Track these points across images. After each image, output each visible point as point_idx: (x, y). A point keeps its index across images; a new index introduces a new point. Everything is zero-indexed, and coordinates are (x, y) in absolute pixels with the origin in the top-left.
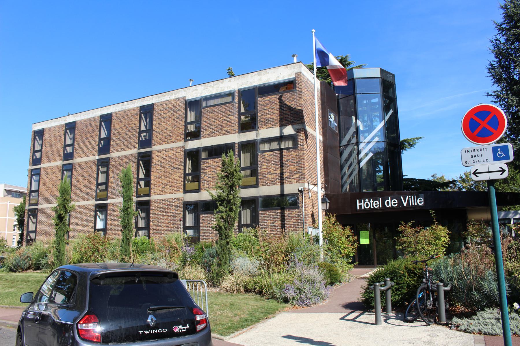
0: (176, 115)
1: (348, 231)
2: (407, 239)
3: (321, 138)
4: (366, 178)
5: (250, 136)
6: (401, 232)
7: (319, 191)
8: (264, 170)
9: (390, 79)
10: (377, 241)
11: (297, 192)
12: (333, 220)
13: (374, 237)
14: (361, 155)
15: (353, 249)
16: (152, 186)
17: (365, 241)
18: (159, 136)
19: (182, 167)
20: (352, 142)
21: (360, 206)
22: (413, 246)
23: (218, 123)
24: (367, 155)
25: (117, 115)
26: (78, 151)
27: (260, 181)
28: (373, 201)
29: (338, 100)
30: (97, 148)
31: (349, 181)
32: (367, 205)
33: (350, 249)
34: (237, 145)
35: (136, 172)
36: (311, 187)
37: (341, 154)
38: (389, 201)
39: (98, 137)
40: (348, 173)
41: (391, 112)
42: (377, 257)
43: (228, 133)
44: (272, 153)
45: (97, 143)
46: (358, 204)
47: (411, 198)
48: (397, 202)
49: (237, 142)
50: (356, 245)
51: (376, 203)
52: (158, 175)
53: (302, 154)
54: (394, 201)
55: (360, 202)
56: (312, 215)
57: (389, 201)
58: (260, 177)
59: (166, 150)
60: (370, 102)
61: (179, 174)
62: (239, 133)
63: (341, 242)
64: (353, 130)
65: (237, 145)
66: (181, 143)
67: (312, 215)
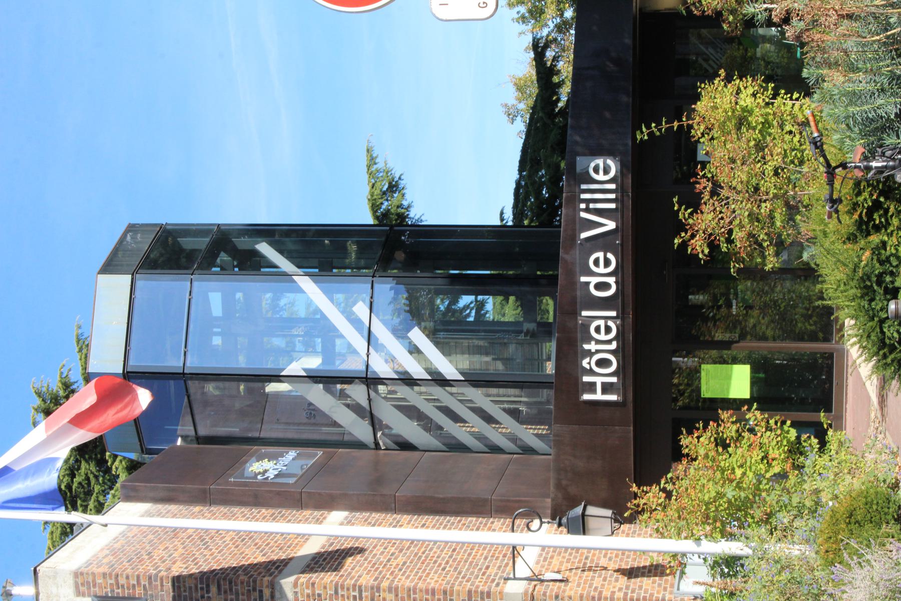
1: (698, 444)
2: (741, 226)
3: (337, 516)
4: (506, 361)
6: (713, 246)
7: (540, 539)
9: (144, 243)
10: (743, 337)
12: (652, 496)
13: (726, 345)
14: (417, 371)
15: (768, 428)
17: (738, 381)
20: (364, 403)
21: (606, 388)
22: (765, 208)
24: (414, 350)
28: (589, 339)
29: (200, 440)
31: (509, 424)
32: (602, 363)
33: (768, 437)
36: (522, 570)
37: (405, 446)
38: (594, 280)
40: (478, 424)
41: (265, 248)
42: (800, 338)
46: (599, 396)
47: (588, 201)
48: (600, 255)
50: (754, 416)
51: (598, 329)
54: (596, 262)
55: (591, 387)
56: (631, 573)
57: (594, 280)
60: (220, 321)
63: (739, 472)
64: (317, 395)
67: (631, 573)
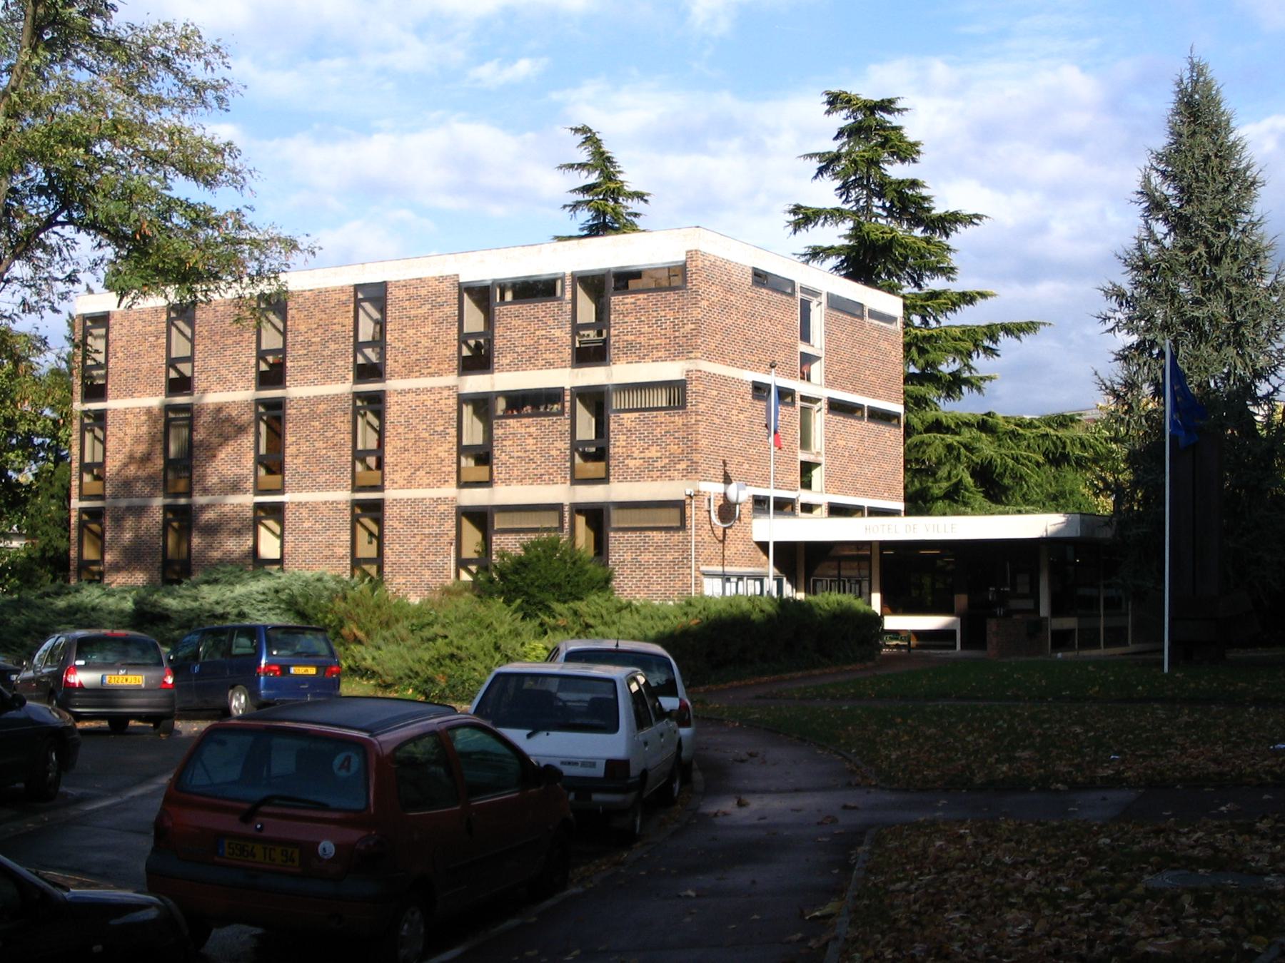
0: (438, 314)
5: (593, 376)
8: (620, 450)
11: (683, 497)
16: (387, 469)
18: (400, 358)
19: (453, 432)
23: (528, 342)
25: (300, 300)
26: (204, 376)
27: (612, 472)
30: (252, 374)
34: (568, 393)
35: (350, 436)
39: (254, 346)
43: (550, 365)
44: (637, 415)
45: (253, 361)
49: (567, 387)
52: (400, 444)
53: (693, 421)
58: (612, 462)
59: (417, 392)
61: (446, 446)
62: (573, 367)
65: (568, 393)
66: (451, 379)
